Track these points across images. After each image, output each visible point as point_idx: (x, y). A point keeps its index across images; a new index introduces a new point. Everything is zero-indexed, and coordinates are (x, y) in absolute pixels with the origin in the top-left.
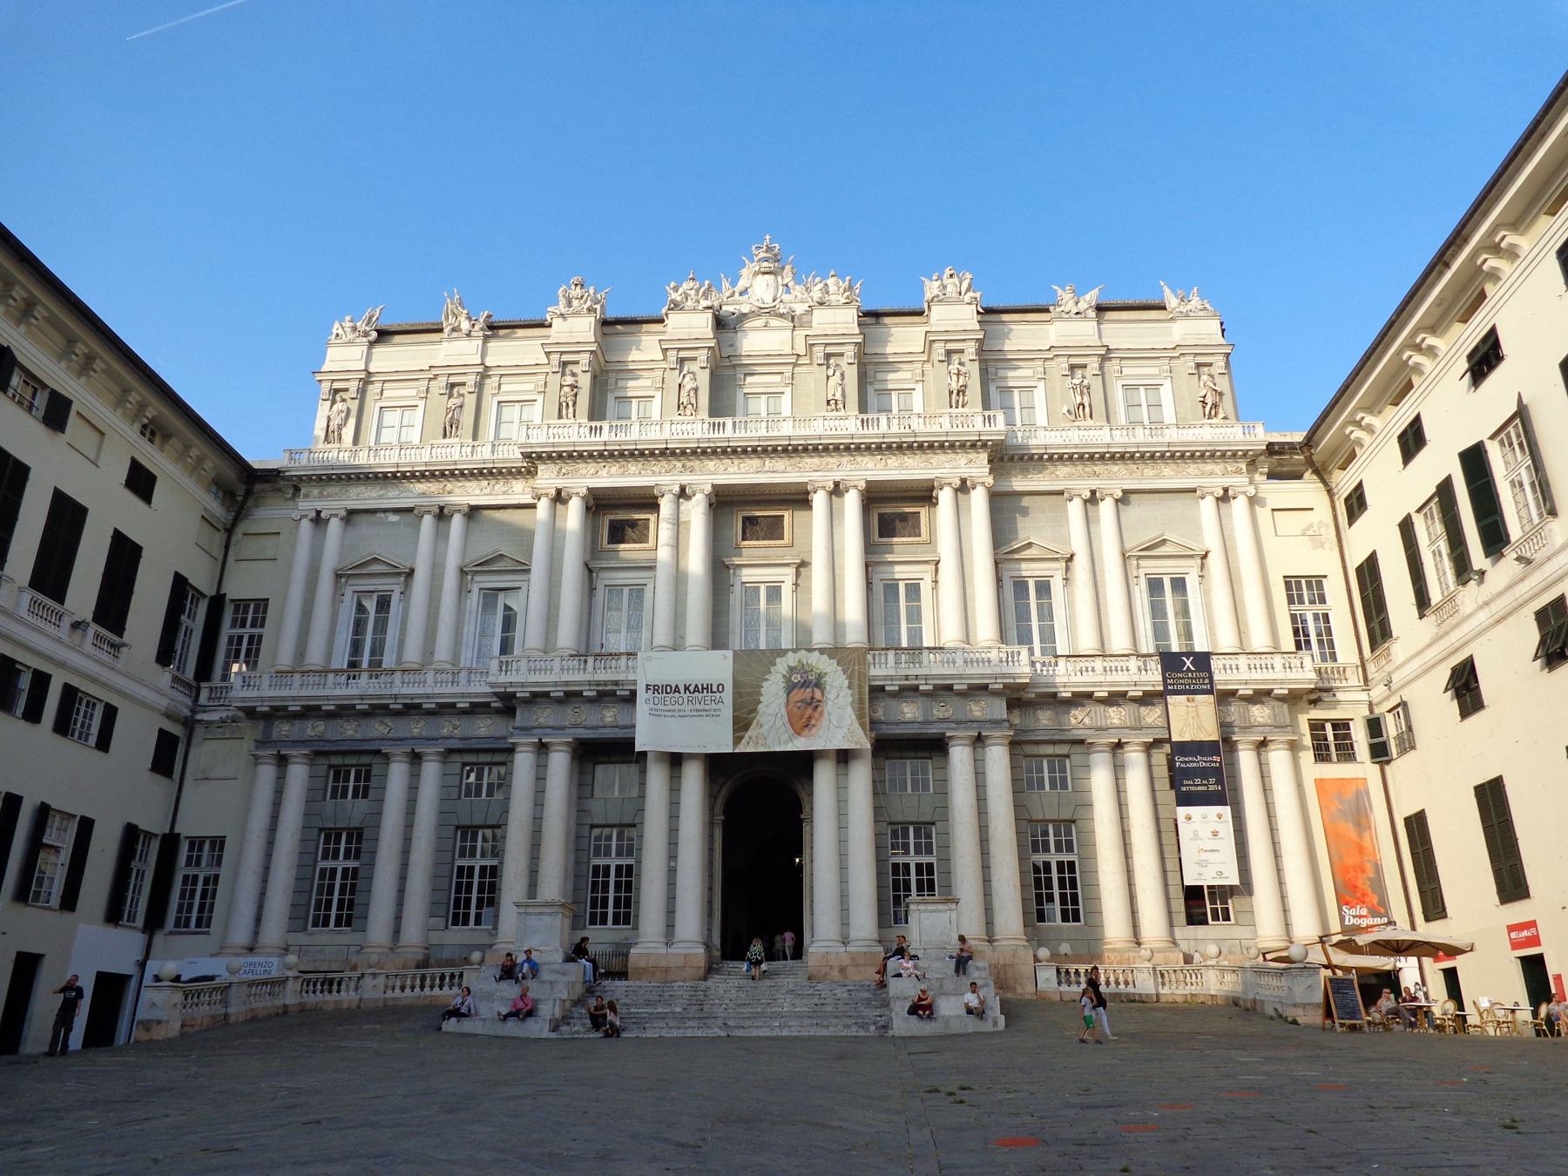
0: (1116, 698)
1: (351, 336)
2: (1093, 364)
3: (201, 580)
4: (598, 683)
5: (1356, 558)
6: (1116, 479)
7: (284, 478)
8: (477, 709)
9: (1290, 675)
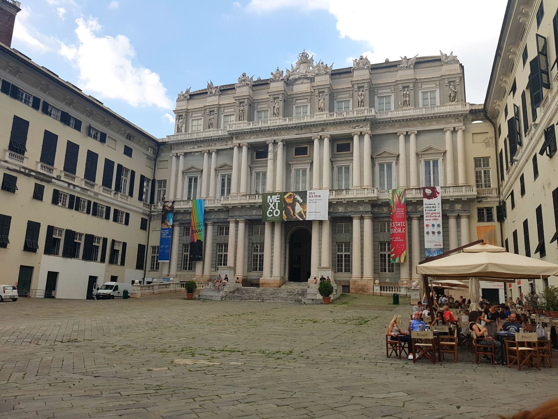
1: (182, 98)
2: (411, 85)
3: (149, 175)
4: (250, 203)
8: (220, 211)
9: (468, 193)
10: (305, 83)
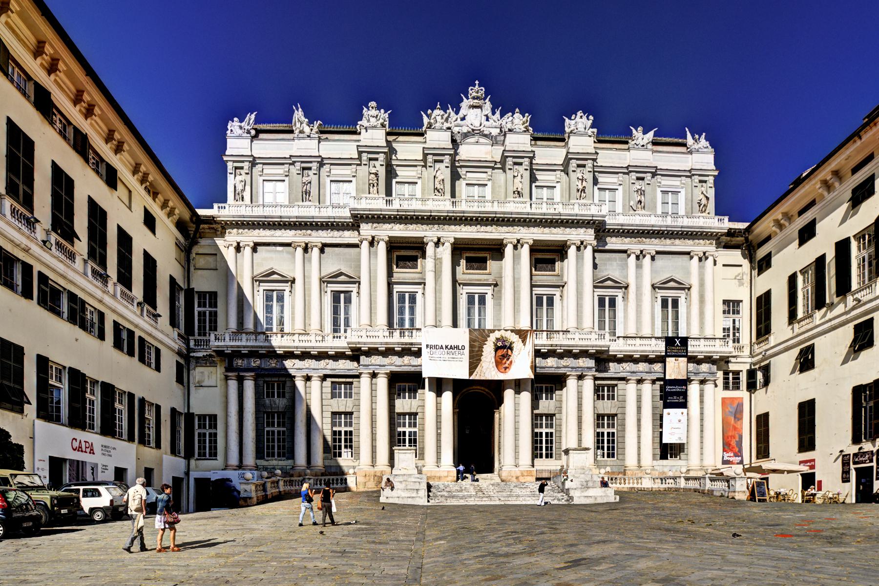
0: (645, 359)
1: (240, 132)
5: (760, 291)
6: (652, 245)
7: (216, 222)
8: (339, 356)
10: (483, 144)
